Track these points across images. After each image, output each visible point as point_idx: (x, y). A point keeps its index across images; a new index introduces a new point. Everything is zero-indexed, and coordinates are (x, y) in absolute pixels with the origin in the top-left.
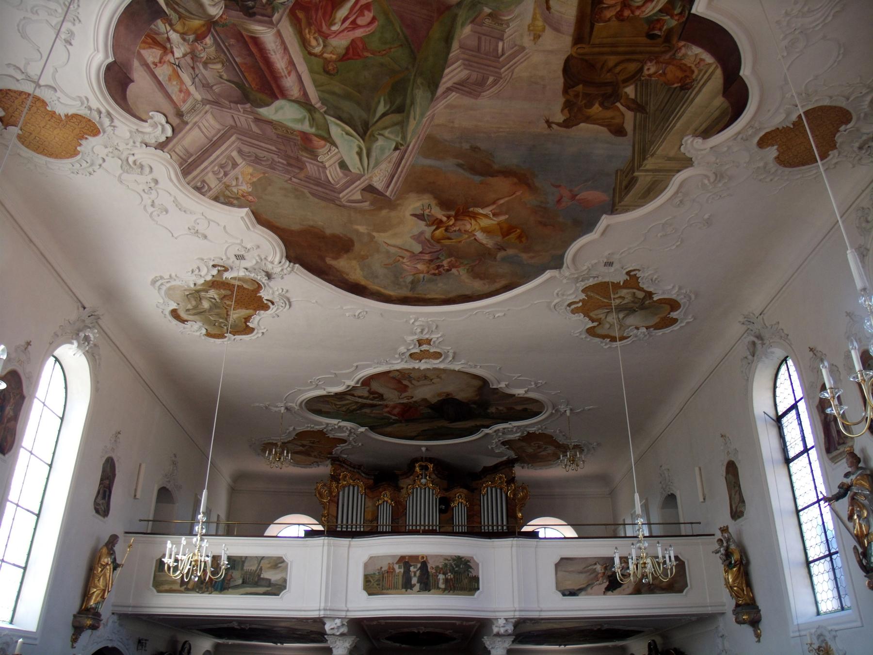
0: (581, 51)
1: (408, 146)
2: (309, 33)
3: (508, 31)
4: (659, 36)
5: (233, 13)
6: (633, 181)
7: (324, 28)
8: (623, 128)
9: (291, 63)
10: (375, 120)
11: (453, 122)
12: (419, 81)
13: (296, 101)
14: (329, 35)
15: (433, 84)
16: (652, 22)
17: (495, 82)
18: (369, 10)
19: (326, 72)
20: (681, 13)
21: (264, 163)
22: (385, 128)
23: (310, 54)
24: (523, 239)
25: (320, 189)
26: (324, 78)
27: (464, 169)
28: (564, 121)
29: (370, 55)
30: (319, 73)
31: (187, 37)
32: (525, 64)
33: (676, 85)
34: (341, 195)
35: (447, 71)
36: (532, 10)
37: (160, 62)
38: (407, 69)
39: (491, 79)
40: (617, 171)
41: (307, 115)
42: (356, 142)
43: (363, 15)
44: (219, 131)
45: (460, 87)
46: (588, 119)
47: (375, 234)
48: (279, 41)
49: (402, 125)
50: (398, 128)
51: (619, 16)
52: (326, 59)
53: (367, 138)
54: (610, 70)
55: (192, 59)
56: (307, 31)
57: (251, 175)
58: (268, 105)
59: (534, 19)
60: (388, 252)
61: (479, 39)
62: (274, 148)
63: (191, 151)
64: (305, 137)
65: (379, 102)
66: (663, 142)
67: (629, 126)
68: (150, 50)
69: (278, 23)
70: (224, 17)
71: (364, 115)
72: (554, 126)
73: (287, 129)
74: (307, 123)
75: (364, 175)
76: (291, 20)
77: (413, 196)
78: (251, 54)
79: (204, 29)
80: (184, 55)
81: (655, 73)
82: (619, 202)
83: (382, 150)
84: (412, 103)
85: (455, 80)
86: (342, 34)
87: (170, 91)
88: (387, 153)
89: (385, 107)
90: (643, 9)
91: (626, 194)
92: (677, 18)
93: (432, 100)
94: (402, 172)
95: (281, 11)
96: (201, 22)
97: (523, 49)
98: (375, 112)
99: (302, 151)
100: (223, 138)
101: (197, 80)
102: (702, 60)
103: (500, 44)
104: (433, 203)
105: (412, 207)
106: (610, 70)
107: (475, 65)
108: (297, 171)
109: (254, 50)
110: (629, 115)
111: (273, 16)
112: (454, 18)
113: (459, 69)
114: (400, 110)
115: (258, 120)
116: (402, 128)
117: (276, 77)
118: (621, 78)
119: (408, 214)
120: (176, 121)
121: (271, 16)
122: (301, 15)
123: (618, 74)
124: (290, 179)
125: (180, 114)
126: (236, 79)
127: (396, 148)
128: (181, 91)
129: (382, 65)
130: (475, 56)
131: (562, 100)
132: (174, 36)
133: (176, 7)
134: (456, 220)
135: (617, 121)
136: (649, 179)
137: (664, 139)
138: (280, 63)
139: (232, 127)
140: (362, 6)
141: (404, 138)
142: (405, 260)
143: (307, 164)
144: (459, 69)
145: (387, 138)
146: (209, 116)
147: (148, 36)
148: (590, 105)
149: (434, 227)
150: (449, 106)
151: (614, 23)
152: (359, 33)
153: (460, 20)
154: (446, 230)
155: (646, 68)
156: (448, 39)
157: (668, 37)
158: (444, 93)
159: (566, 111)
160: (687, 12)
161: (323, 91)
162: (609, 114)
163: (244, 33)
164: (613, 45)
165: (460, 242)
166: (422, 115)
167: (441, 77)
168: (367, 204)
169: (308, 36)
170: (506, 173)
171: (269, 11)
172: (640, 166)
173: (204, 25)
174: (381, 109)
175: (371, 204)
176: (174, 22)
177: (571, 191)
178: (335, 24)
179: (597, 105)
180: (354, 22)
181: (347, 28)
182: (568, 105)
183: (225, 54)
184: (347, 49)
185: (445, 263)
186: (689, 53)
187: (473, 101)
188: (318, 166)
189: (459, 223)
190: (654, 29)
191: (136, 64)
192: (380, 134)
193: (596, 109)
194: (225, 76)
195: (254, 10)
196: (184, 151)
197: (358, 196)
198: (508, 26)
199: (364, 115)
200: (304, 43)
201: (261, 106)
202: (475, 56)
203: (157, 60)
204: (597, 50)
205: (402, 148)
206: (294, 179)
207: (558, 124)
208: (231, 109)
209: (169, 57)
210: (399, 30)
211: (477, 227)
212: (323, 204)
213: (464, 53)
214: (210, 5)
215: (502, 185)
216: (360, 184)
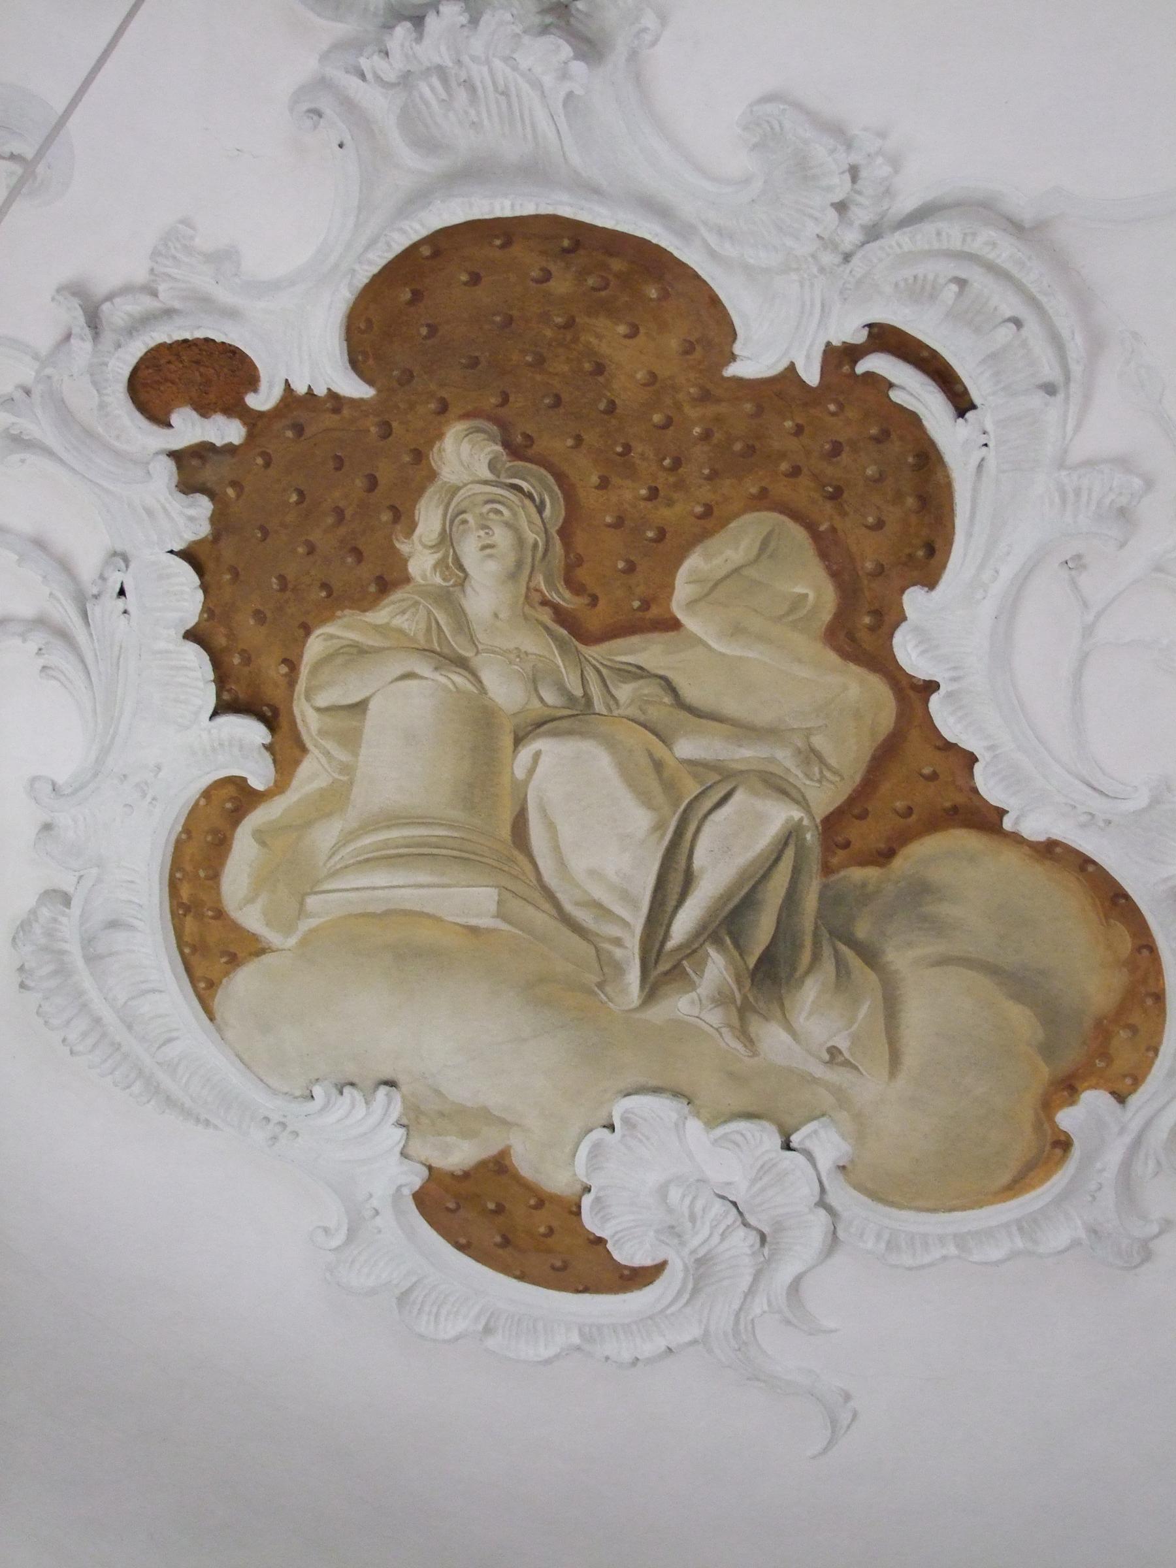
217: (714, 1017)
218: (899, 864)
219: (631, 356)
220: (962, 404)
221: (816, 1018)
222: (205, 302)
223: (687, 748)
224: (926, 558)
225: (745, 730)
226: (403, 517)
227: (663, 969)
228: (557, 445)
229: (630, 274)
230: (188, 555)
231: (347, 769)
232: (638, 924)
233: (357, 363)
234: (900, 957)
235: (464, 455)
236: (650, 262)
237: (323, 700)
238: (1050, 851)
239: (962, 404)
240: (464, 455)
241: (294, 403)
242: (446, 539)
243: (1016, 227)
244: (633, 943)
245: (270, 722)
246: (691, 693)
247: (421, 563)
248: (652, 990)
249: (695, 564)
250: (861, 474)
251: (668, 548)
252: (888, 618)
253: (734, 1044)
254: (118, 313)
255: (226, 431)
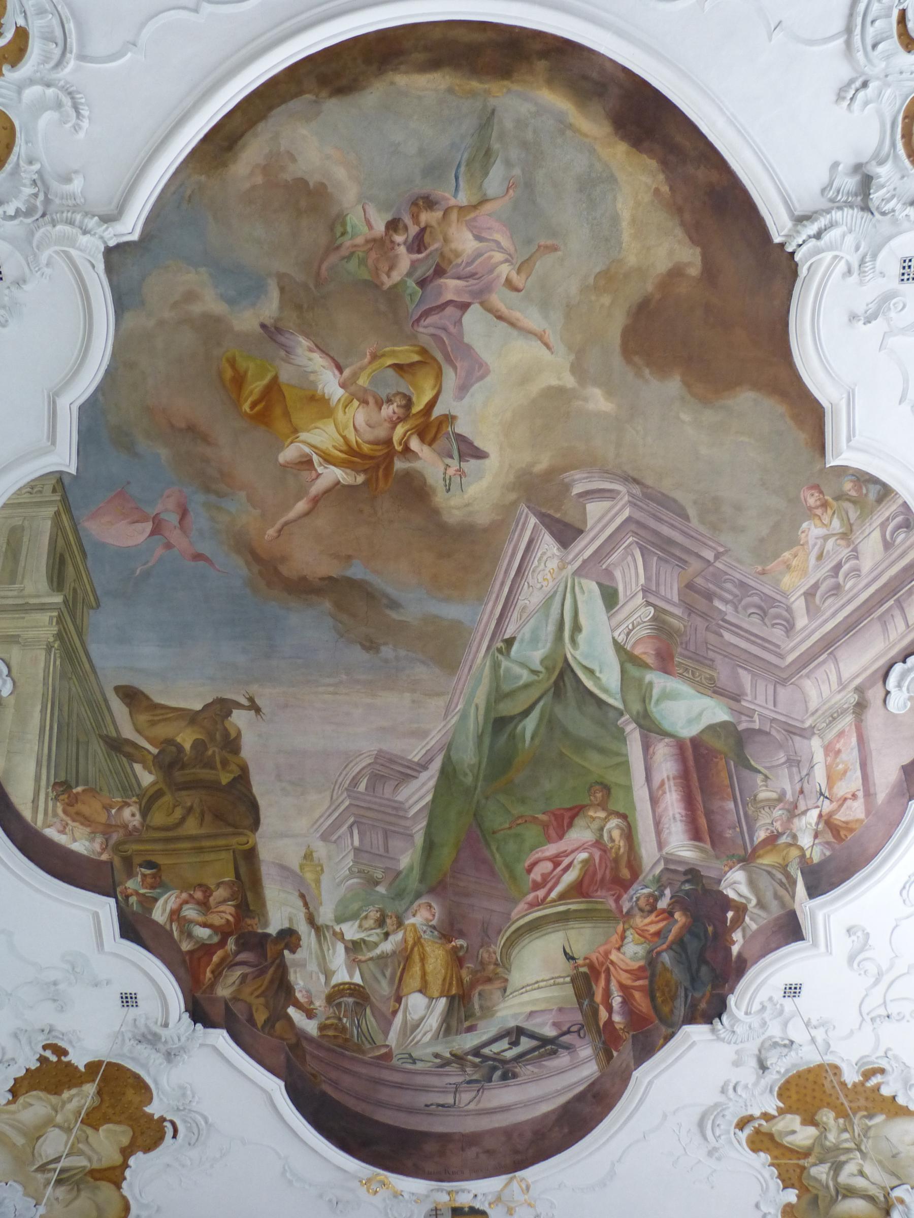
0: (243, 839)
1: (489, 648)
2: (619, 849)
3: (349, 862)
4: (141, 866)
5: (713, 874)
6: (57, 576)
7: (597, 855)
8: (128, 705)
9: (654, 801)
10: (541, 703)
11: (413, 701)
12: (469, 780)
13: (665, 734)
14: (593, 845)
15: (448, 774)
16: (158, 883)
17: (355, 782)
18: (534, 882)
19: (607, 789)
20: (127, 897)
21: (756, 599)
22: (527, 686)
23: (624, 817)
24: (229, 373)
25: (665, 530)
26: (612, 777)
27: (387, 596)
28: (229, 714)
29: (540, 816)
30: (616, 784)
31: (789, 840)
32: (317, 814)
33: (79, 789)
34: (626, 513)
35: (429, 798)
36: (323, 893)
37: (846, 799)
38: (487, 798)
39: (362, 787)
40: (98, 606)
41: (653, 709)
42: (577, 655)
43: (543, 875)
44: (808, 676)
45: (407, 772)
46: (192, 718)
47: (570, 381)
48: (664, 835)
49: (498, 695)
50: (506, 688)
51: (207, 892)
52: (603, 809)
53: (560, 665)
54: (190, 810)
55: (796, 807)
56: (622, 850)
57: (789, 567)
58: (712, 728)
59: (318, 882)
60: (545, 306)
61: (387, 851)
62: (727, 636)
63: (877, 628)
64: (665, 662)
65: (532, 738)
66: (46, 678)
67: (118, 707)
68: (851, 818)
69: (658, 861)
70: (727, 869)
71: (559, 711)
72: (245, 702)
73: (693, 682)
74: (656, 692)
75: (577, 573)
76: (640, 866)
77: (483, 517)
78: (708, 814)
79: (761, 852)
80: (804, 813)
81: (120, 809)
82: (57, 514)
83: (535, 640)
84: (480, 737)
85: (414, 784)
86: (576, 846)
87: (855, 753)
88: (527, 630)
89: (524, 729)
90: (179, 901)
91: (53, 542)
92: (129, 891)
93: (449, 747)
94: (503, 584)
95: (650, 877)
96: (760, 861)
97: (325, 837)
98: (541, 719)
99: (678, 631)
100: (807, 660)
101: (804, 772)
102: (62, 832)
103: (357, 843)
104: (440, 498)
105: (484, 483)
106: (190, 810)
107: (389, 811)
108: (699, 581)
109: (703, 822)
110: (128, 732)
111: (662, 871)
112: (423, 879)
113: (411, 802)
114: (500, 724)
115: (733, 697)
116: (498, 688)
117: (684, 778)
118: (167, 798)
119: (492, 463)
120: (874, 694)
121: (666, 869)
122: (625, 873)
123: (175, 806)
124: (717, 556)
125: (861, 707)
126: (746, 773)
127: (510, 642)
128: (839, 751)
129: (523, 801)
130: (390, 823)
131: (247, 753)
132: (806, 841)
133: (784, 880)
134: (389, 442)
135: (143, 718)
136: (29, 587)
137: (45, 683)
138: (672, 802)
139: (784, 682)
140: (543, 887)
141: (496, 666)
142: (505, 270)
143: (676, 599)
144: (411, 802)
145: (523, 665)
146: (813, 704)
147: (843, 840)
148: (198, 745)
149: (437, 412)
150: (422, 734)
151: (211, 883)
152: (551, 849)
153: (416, 874)
154: (408, 404)
155: (138, 817)
156: (430, 847)
157: (128, 863)
158: (431, 760)
159: (233, 735)
160: (120, 898)
161: (618, 754)
162: (163, 731)
163: (708, 846)
164: (200, 850)
165: (375, 357)
166: (464, 716)
167: (437, 787)
168: (577, 489)
169: (622, 844)
170: (303, 589)
171: (664, 879)
172: (60, 620)
173: (759, 857)
174: (530, 724)
175: (567, 487)
176: (797, 860)
177: (169, 546)
178: (582, 862)
179: (187, 746)
180: (556, 864)
181: (567, 856)
182: (232, 744)
183: (746, 814)
184: (570, 825)
185: (405, 259)
186: (87, 843)
187: (385, 747)
188: (656, 594)
189: (381, 433)
190: (154, 876)
191: (881, 796)
192: (534, 672)
193: (187, 739)
194: (759, 779)
195: (683, 878)
196: (890, 627)
197: (594, 509)
198: (350, 869)
199: (559, 711)
200: (629, 834)
201: (724, 725)
202: (390, 823)
203: (849, 802)
204: (221, 842)
205: (500, 644)
206: (709, 555)
207: (239, 706)
208: (773, 720)
209: (827, 807)
210: (497, 856)
211: (340, 414)
212: (666, 486)
213: (407, 828)
214: (739, 883)
215: (308, 559)
216: (585, 547)
217: (42, 1181)
218: (98, 1183)
219: (130, 1094)
220: (174, 1137)
221: (61, 1192)
222: (70, 1042)
223: (81, 1146)
224: (148, 1149)
225: (93, 1150)
226: (69, 1088)
227: (42, 1169)
228: (106, 1098)
229: (143, 1089)
230: (27, 1070)
231: (19, 1111)
232: (45, 1161)
233: (86, 1066)
234: (83, 1194)
235: (90, 1089)
236: (147, 1088)
237: (27, 1100)
238: (124, 1198)
239: (174, 1137)
240: (90, 1089)
241: (69, 1064)
242: (74, 1096)
243: (206, 1122)
244: (41, 1163)
245: (13, 1097)
246: (90, 1139)
247: (66, 1095)
248: (37, 1170)
249: (110, 1126)
250: (150, 1134)
251: (108, 1121)
252: (132, 1153)
253: (42, 1187)
254: (54, 1033)
255: (54, 1059)
